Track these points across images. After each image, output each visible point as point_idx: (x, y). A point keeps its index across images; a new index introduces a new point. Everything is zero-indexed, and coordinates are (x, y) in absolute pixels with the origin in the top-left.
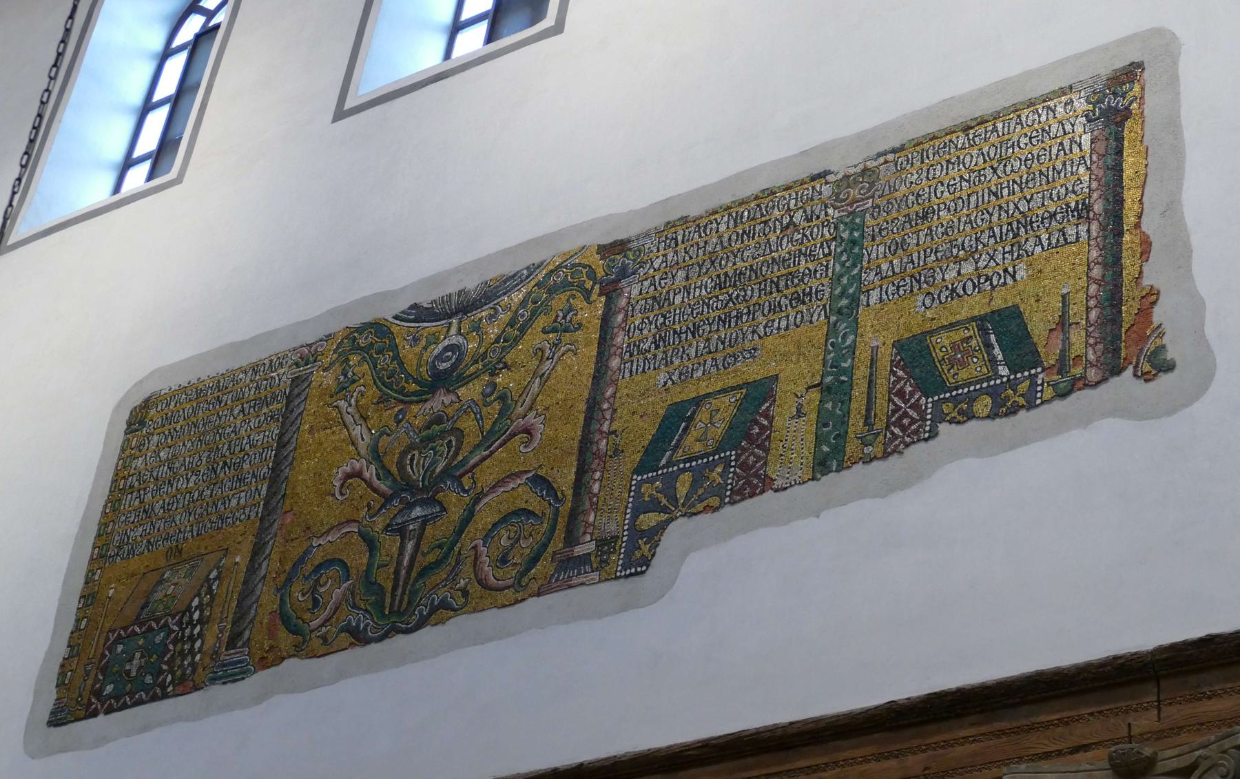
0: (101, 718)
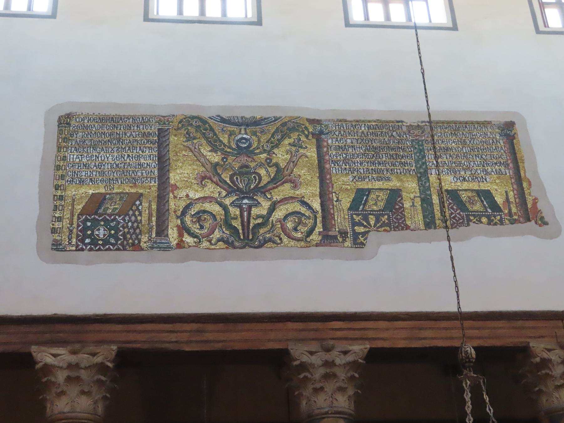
0: (86, 252)
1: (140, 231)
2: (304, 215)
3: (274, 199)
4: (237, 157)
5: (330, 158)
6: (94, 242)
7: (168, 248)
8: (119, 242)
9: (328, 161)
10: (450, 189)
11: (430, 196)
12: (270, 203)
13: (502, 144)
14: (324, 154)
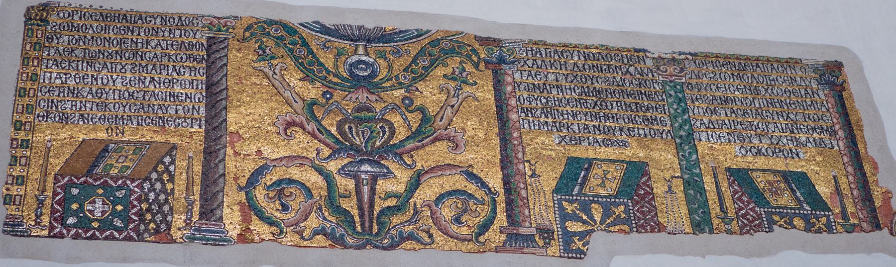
0: (67, 241)
1: (171, 209)
2: (471, 196)
3: (419, 165)
4: (350, 92)
5: (519, 103)
6: (84, 224)
7: (221, 241)
8: (131, 226)
9: (514, 108)
10: (735, 167)
11: (699, 178)
12: (410, 173)
13: (823, 97)
14: (508, 96)
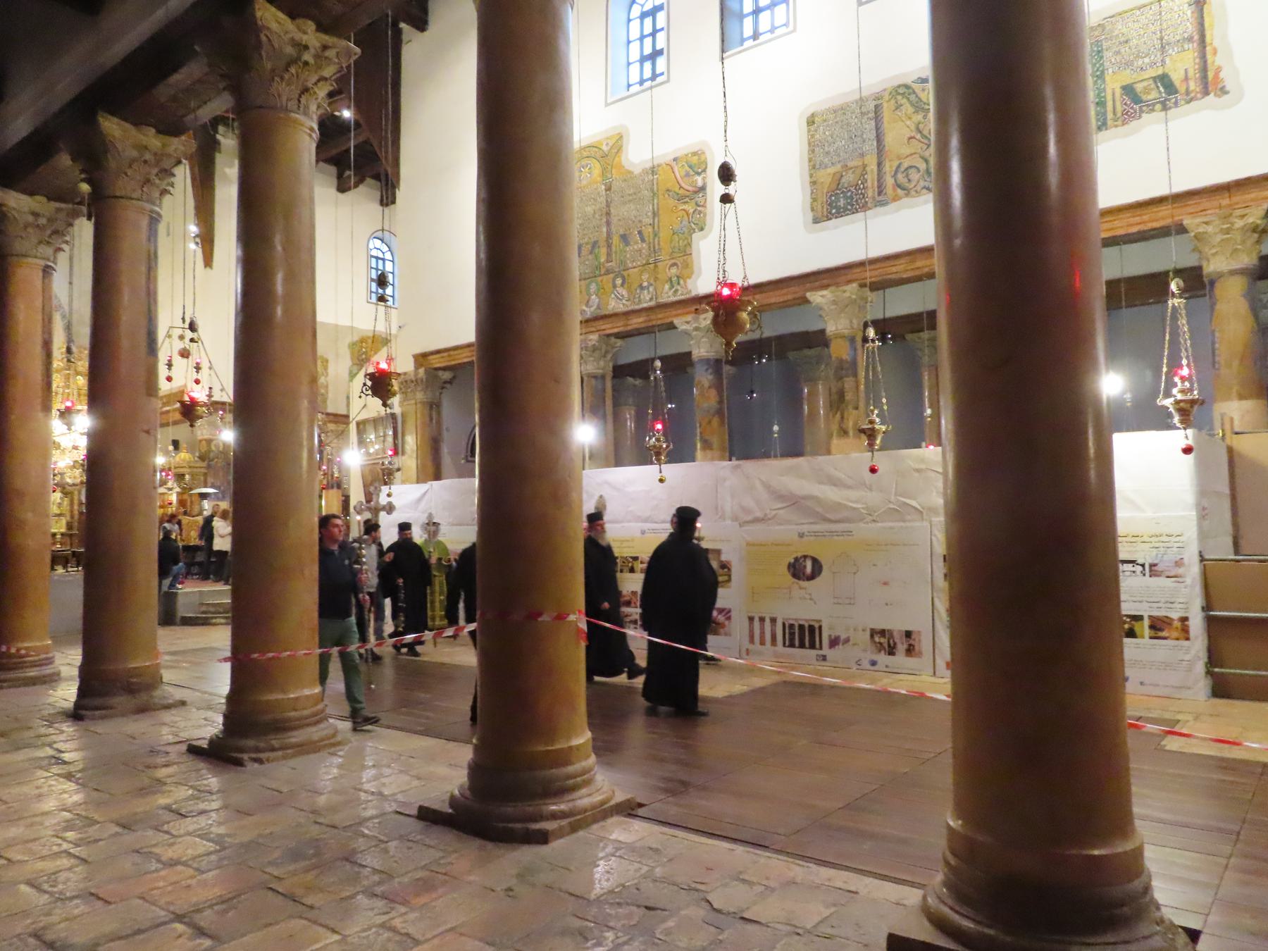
0: (834, 220)
